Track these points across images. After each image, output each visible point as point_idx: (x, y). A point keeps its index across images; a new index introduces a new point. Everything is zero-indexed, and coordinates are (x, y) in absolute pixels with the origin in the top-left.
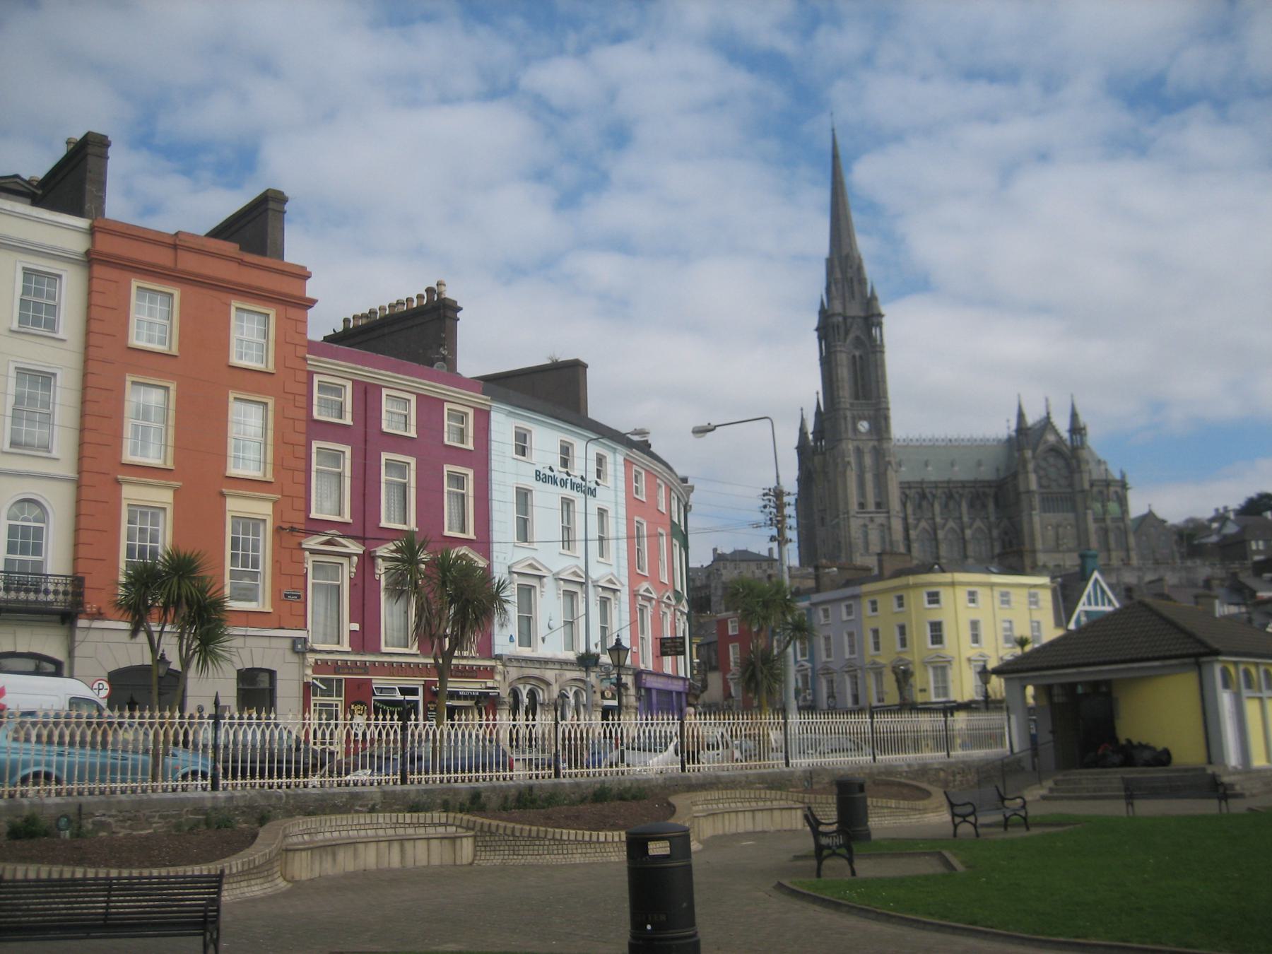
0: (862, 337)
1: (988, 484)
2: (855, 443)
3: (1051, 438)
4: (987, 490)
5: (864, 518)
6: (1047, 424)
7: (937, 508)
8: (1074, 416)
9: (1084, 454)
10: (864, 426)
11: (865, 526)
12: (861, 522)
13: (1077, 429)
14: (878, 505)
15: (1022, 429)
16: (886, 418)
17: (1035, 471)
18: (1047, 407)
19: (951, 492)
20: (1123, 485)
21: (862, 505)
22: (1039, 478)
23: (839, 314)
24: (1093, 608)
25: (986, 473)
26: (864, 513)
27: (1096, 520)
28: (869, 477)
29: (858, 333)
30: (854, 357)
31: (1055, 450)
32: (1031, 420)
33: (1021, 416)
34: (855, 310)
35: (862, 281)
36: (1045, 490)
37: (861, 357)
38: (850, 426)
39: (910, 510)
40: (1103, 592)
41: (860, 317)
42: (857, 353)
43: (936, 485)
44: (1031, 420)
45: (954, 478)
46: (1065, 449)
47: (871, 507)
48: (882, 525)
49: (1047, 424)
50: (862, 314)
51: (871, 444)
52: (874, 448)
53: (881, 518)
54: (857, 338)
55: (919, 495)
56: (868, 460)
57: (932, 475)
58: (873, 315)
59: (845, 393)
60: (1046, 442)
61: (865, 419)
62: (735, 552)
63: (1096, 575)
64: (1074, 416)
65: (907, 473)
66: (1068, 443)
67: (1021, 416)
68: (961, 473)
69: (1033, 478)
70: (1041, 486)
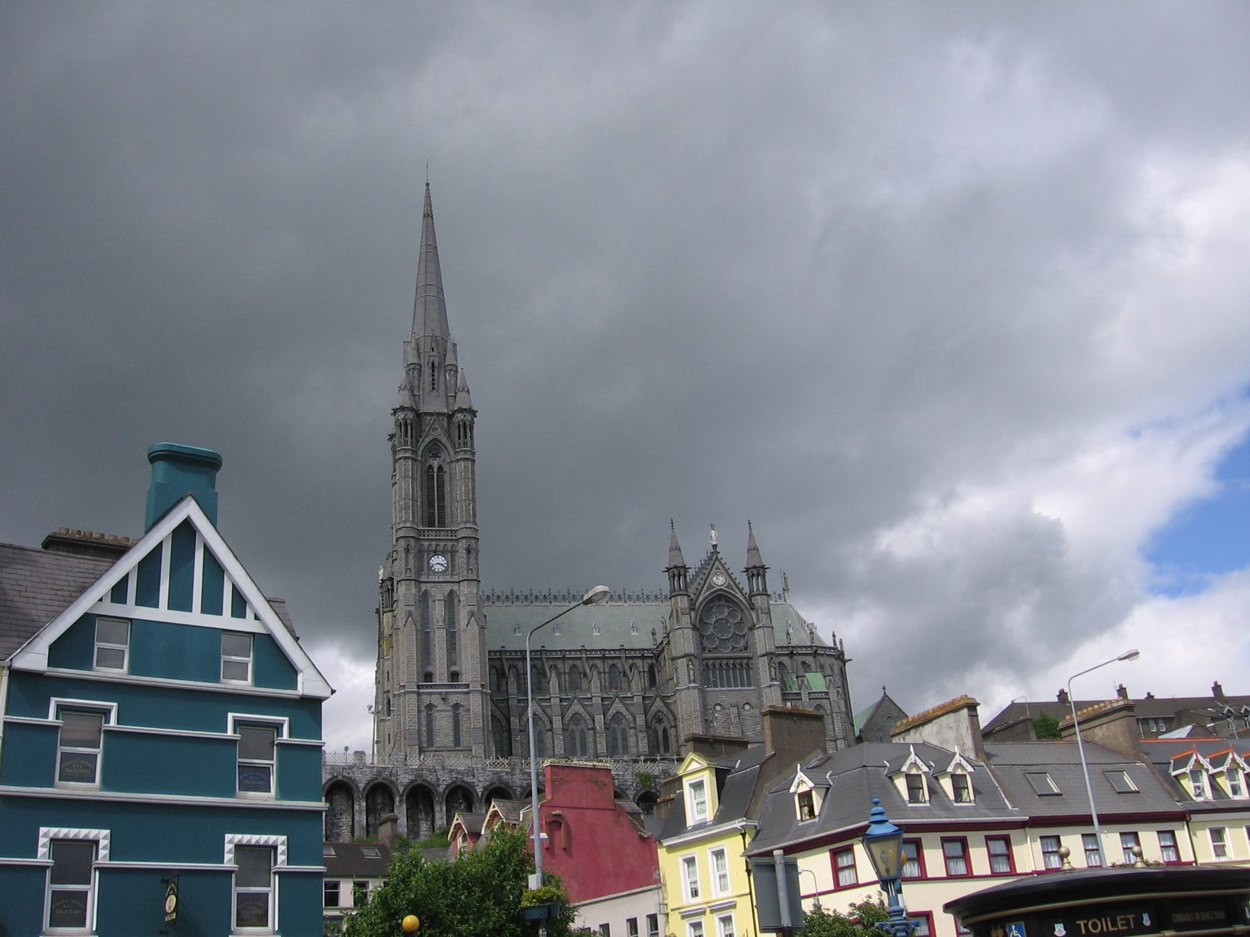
0: (444, 440)
2: (424, 587)
3: (719, 580)
4: (639, 662)
5: (430, 694)
11: (430, 707)
13: (756, 571)
14: (454, 676)
17: (694, 628)
23: (411, 409)
24: (162, 613)
26: (431, 687)
30: (431, 467)
31: (721, 597)
32: (693, 558)
34: (433, 404)
37: (440, 468)
40: (215, 568)
41: (439, 414)
42: (435, 464)
44: (693, 558)
46: (739, 595)
47: (441, 677)
48: (456, 706)
50: (445, 410)
51: (448, 588)
52: (452, 592)
54: (436, 442)
58: (461, 410)
60: (710, 587)
61: (443, 553)
64: (753, 549)
66: (747, 590)
69: (689, 633)
70: (704, 649)
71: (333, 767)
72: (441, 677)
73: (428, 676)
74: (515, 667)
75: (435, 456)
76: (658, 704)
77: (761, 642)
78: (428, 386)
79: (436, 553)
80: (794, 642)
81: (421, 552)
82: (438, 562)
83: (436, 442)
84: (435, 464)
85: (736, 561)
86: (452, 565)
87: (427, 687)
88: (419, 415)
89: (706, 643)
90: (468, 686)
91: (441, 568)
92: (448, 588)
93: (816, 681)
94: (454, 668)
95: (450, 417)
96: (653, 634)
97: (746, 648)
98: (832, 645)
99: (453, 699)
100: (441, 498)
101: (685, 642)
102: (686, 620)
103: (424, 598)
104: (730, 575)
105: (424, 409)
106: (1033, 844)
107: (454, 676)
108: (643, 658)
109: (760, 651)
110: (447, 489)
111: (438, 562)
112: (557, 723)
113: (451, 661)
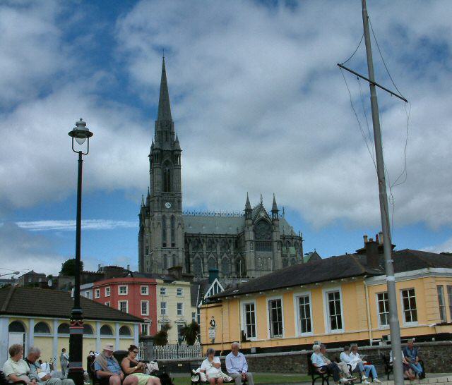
0: (171, 161)
1: (233, 236)
2: (163, 214)
3: (262, 214)
4: (232, 239)
6: (261, 207)
7: (204, 247)
8: (274, 204)
9: (280, 223)
13: (275, 211)
14: (173, 245)
15: (248, 210)
16: (180, 202)
17: (254, 231)
19: (212, 240)
20: (301, 239)
21: (165, 245)
22: (255, 234)
23: (159, 149)
25: (233, 231)
27: (282, 256)
28: (169, 231)
29: (168, 158)
31: (264, 220)
32: (253, 205)
33: (248, 203)
34: (167, 147)
35: (173, 133)
37: (169, 170)
38: (160, 205)
39: (191, 248)
43: (206, 236)
44: (253, 205)
45: (215, 233)
47: (169, 246)
48: (174, 255)
49: (261, 207)
51: (171, 214)
53: (174, 252)
54: (167, 161)
55: (193, 241)
56: (168, 222)
57: (205, 231)
58: (176, 150)
59: (159, 188)
62: (82, 263)
63: (216, 280)
64: (274, 204)
65: (191, 230)
66: (271, 217)
67: (248, 203)
68: (219, 230)
69: (252, 233)
70: (256, 238)
72: (169, 246)
73: (165, 245)
76: (239, 255)
77: (276, 237)
78: (164, 140)
79: (167, 201)
80: (286, 234)
81: (162, 201)
82: (168, 205)
84: (167, 169)
85: (268, 207)
86: (173, 207)
88: (162, 151)
91: (169, 207)
92: (171, 214)
93: (292, 250)
95: (173, 152)
97: (270, 238)
99: (173, 253)
100: (169, 182)
101: (250, 235)
102: (251, 228)
103: (164, 217)
107: (173, 245)
108: (233, 238)
109: (275, 239)
110: (171, 178)
112: (206, 261)
113: (173, 240)
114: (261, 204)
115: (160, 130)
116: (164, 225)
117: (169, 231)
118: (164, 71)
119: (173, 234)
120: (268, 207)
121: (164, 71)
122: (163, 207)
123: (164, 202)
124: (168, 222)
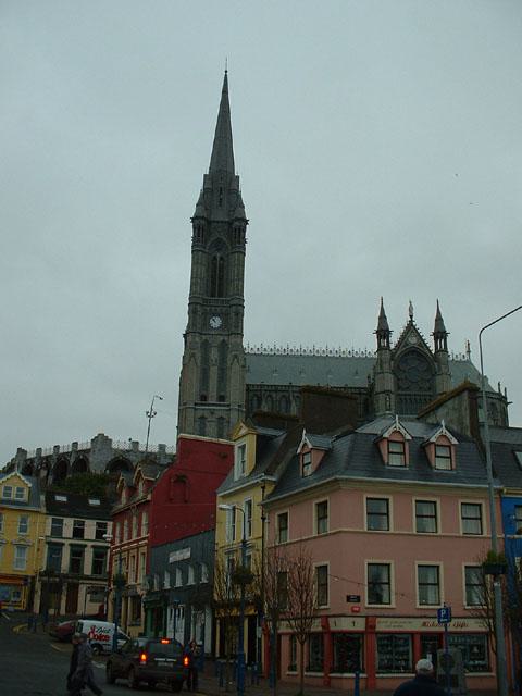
0: (225, 239)
3: (413, 340)
6: (411, 328)
8: (439, 320)
10: (216, 322)
12: (200, 414)
13: (440, 334)
14: (222, 398)
16: (239, 315)
18: (411, 309)
21: (204, 398)
22: (397, 380)
28: (214, 372)
30: (215, 258)
33: (383, 318)
36: (400, 392)
37: (221, 258)
41: (222, 222)
47: (212, 399)
49: (411, 328)
52: (224, 341)
53: (220, 411)
54: (219, 241)
56: (214, 354)
58: (237, 219)
64: (439, 320)
66: (432, 348)
67: (383, 318)
70: (399, 388)
71: (116, 450)
72: (212, 399)
73: (204, 398)
74: (270, 396)
75: (219, 250)
78: (216, 203)
83: (219, 241)
87: (202, 405)
88: (209, 222)
89: (401, 384)
90: (229, 405)
94: (222, 393)
95: (230, 224)
96: (369, 378)
98: (497, 391)
99: (219, 414)
101: (388, 382)
104: (421, 337)
105: (212, 218)
106: (85, 538)
107: (222, 398)
111: (216, 322)
114: (411, 321)
115: (210, 187)
116: (206, 359)
117: (214, 372)
118: (225, 92)
119: (223, 378)
120: (426, 331)
121: (225, 92)
122: (206, 324)
123: (207, 316)
124: (214, 354)
